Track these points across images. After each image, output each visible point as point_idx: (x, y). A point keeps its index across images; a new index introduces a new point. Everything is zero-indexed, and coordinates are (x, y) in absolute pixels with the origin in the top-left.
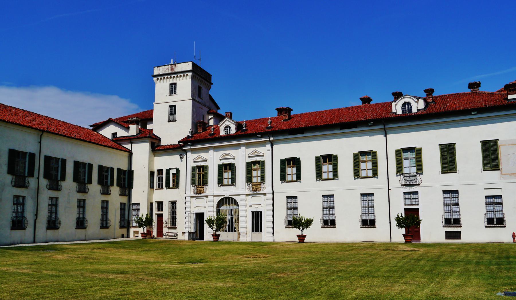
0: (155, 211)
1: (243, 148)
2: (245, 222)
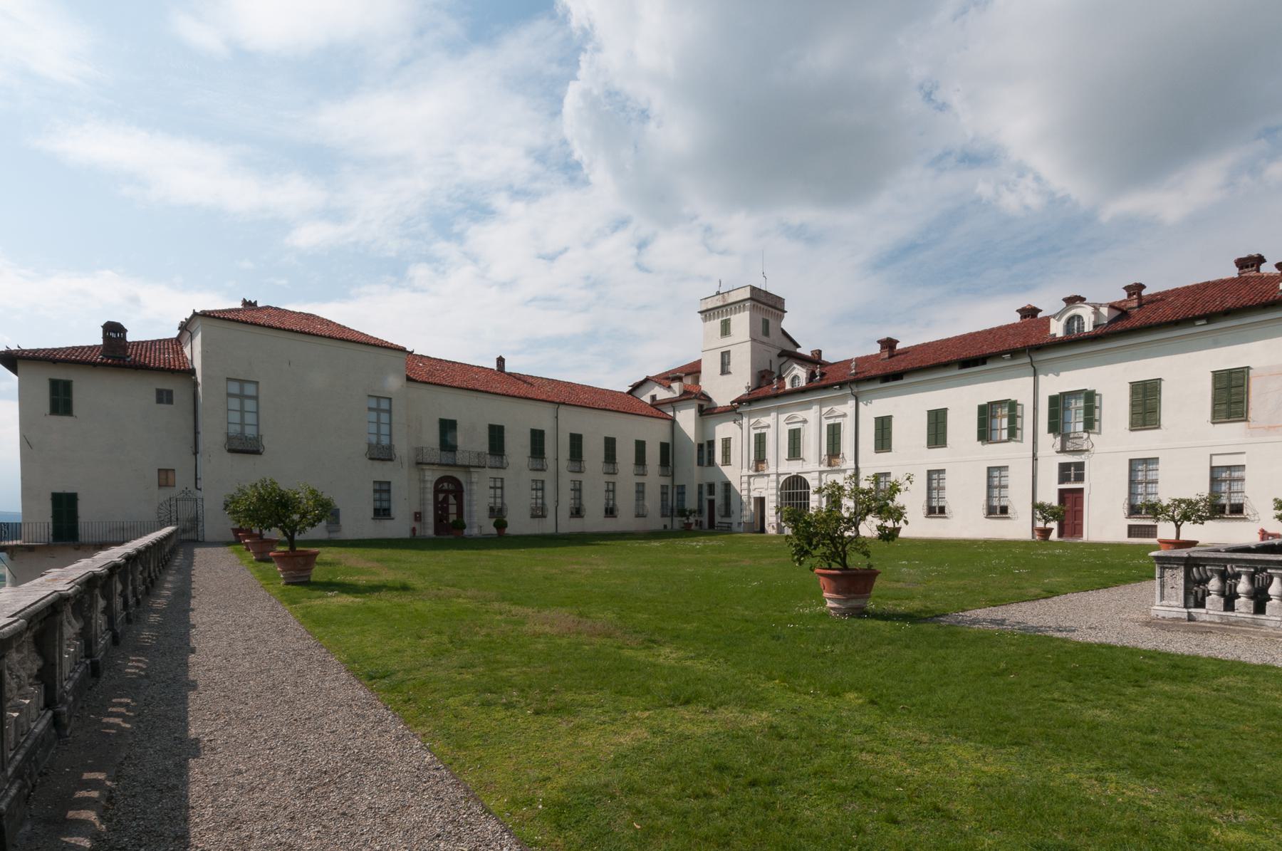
0: (706, 496)
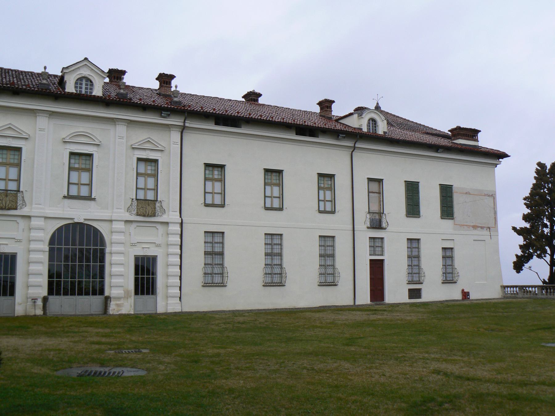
1: (121, 129)
2: (119, 277)
